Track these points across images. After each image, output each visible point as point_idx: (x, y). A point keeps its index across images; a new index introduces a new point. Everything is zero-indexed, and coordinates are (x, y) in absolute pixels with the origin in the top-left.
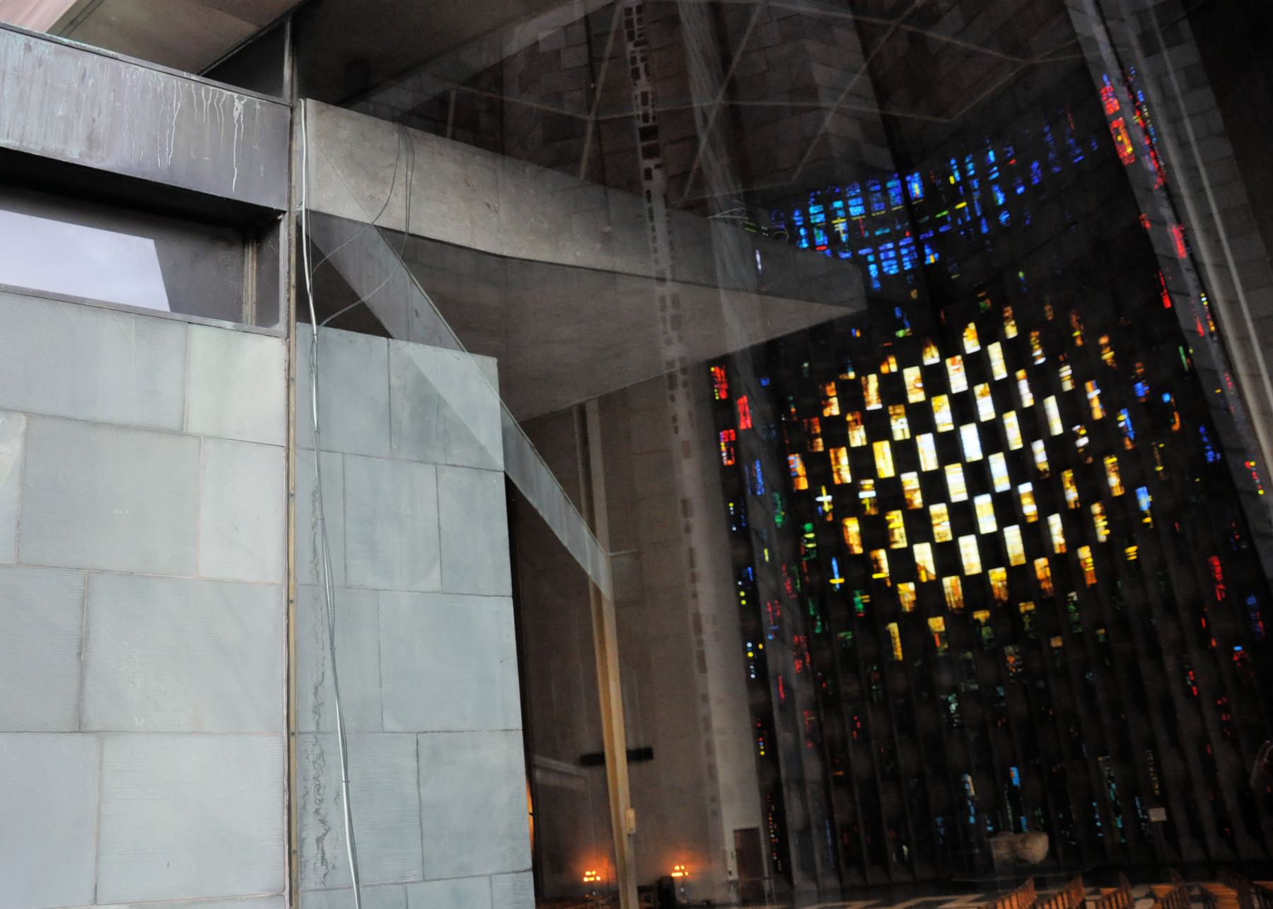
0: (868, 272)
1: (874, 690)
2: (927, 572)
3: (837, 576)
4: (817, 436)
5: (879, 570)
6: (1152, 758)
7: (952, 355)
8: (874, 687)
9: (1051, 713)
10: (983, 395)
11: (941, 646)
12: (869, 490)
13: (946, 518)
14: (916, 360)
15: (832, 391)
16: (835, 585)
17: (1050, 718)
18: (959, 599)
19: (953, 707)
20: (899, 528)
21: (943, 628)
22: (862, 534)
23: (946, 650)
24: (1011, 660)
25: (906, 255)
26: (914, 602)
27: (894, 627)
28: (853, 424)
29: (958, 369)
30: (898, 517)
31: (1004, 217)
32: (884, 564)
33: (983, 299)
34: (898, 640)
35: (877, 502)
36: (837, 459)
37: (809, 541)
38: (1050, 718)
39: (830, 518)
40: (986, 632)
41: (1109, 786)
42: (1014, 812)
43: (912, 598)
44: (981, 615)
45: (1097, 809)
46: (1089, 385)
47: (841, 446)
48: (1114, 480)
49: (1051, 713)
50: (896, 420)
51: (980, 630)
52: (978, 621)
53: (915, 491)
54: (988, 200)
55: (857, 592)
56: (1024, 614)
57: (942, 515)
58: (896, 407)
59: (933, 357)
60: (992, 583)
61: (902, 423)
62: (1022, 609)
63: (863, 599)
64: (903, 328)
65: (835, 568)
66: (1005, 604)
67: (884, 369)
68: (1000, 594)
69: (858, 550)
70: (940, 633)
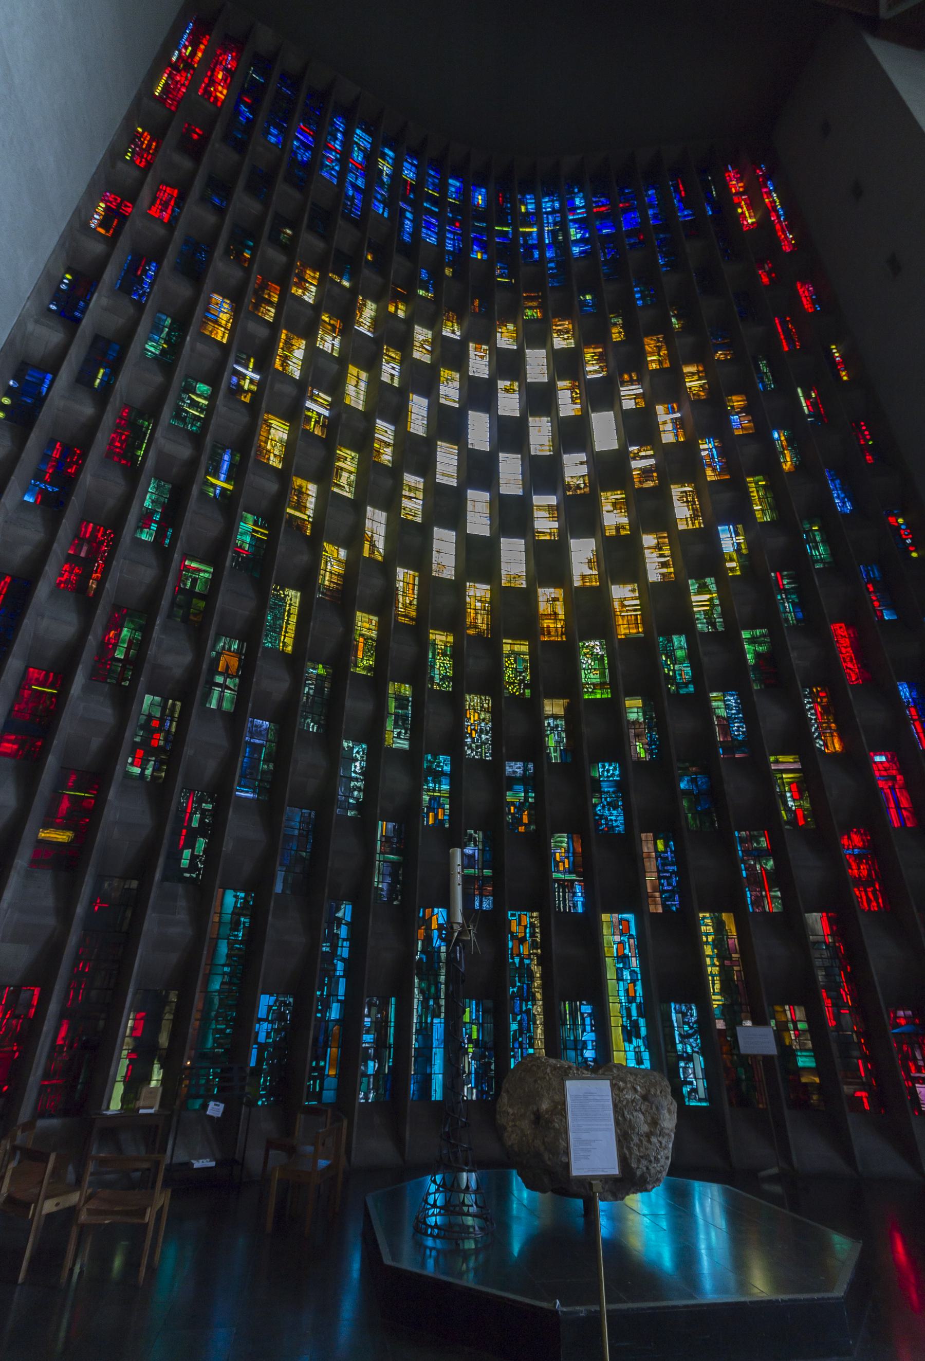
0: (402, 224)
1: (218, 685)
2: (373, 546)
3: (223, 476)
4: (270, 303)
5: (301, 507)
6: (710, 929)
7: (479, 341)
8: (219, 679)
9: (525, 820)
10: (507, 390)
11: (364, 662)
12: (321, 405)
13: (420, 495)
14: (433, 323)
15: (314, 278)
16: (214, 486)
17: (522, 829)
18: (411, 603)
19: (357, 766)
20: (351, 473)
21: (374, 634)
22: (289, 446)
23: (369, 668)
24: (473, 717)
25: (450, 239)
26: (339, 575)
27: (293, 597)
28: (329, 327)
29: (482, 357)
30: (353, 458)
31: (576, 250)
32: (311, 503)
33: (531, 308)
34: (294, 619)
35: (330, 425)
36: (289, 346)
37: (194, 404)
38: (522, 829)
39: (247, 399)
40: (441, 667)
41: (620, 978)
42: (425, 1003)
43: (337, 569)
44: (440, 638)
45: (588, 1021)
46: (660, 409)
47: (301, 336)
48: (682, 512)
49: (525, 820)
50: (388, 363)
51: (433, 657)
52: (434, 644)
53: (387, 445)
54: (563, 226)
55: (250, 518)
56: (508, 656)
57: (416, 489)
58: (391, 350)
59: (453, 332)
60: (468, 600)
61: (393, 368)
62: (506, 648)
63: (254, 530)
64: (427, 291)
65: (225, 467)
66: (480, 635)
67: (392, 309)
68: (475, 618)
69: (275, 463)
70: (366, 638)
